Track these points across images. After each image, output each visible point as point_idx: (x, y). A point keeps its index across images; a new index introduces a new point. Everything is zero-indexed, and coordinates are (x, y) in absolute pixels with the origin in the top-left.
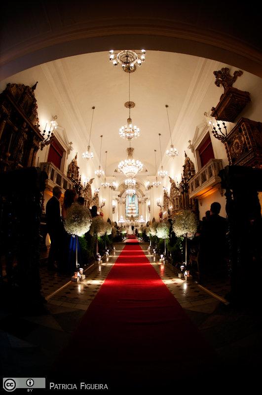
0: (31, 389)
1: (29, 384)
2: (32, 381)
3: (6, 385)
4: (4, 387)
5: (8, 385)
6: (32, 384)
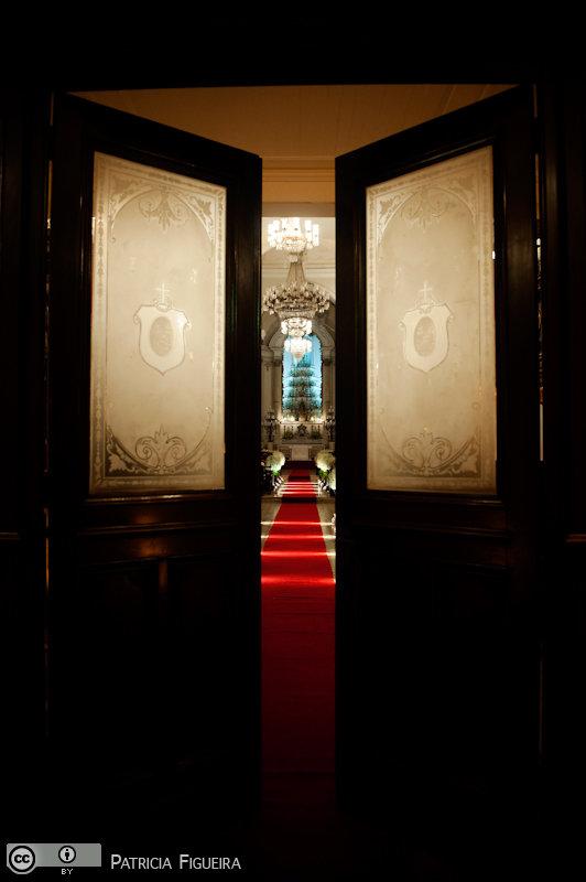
0: (70, 868)
1: (64, 858)
2: (71, 851)
3: (13, 859)
4: (8, 865)
5: (19, 859)
6: (71, 858)
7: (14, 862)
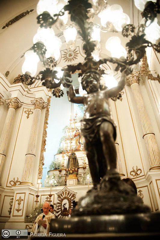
0: (19, 236)
1: (18, 234)
2: (19, 232)
3: (4, 234)
4: (2, 235)
5: (5, 234)
6: (19, 233)
7: (4, 235)
